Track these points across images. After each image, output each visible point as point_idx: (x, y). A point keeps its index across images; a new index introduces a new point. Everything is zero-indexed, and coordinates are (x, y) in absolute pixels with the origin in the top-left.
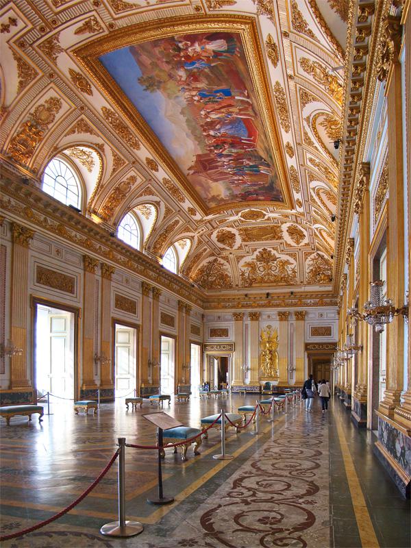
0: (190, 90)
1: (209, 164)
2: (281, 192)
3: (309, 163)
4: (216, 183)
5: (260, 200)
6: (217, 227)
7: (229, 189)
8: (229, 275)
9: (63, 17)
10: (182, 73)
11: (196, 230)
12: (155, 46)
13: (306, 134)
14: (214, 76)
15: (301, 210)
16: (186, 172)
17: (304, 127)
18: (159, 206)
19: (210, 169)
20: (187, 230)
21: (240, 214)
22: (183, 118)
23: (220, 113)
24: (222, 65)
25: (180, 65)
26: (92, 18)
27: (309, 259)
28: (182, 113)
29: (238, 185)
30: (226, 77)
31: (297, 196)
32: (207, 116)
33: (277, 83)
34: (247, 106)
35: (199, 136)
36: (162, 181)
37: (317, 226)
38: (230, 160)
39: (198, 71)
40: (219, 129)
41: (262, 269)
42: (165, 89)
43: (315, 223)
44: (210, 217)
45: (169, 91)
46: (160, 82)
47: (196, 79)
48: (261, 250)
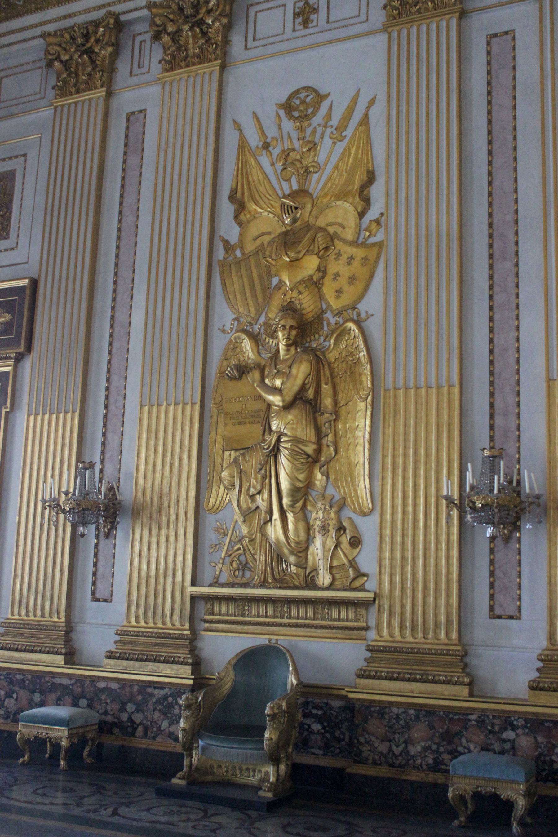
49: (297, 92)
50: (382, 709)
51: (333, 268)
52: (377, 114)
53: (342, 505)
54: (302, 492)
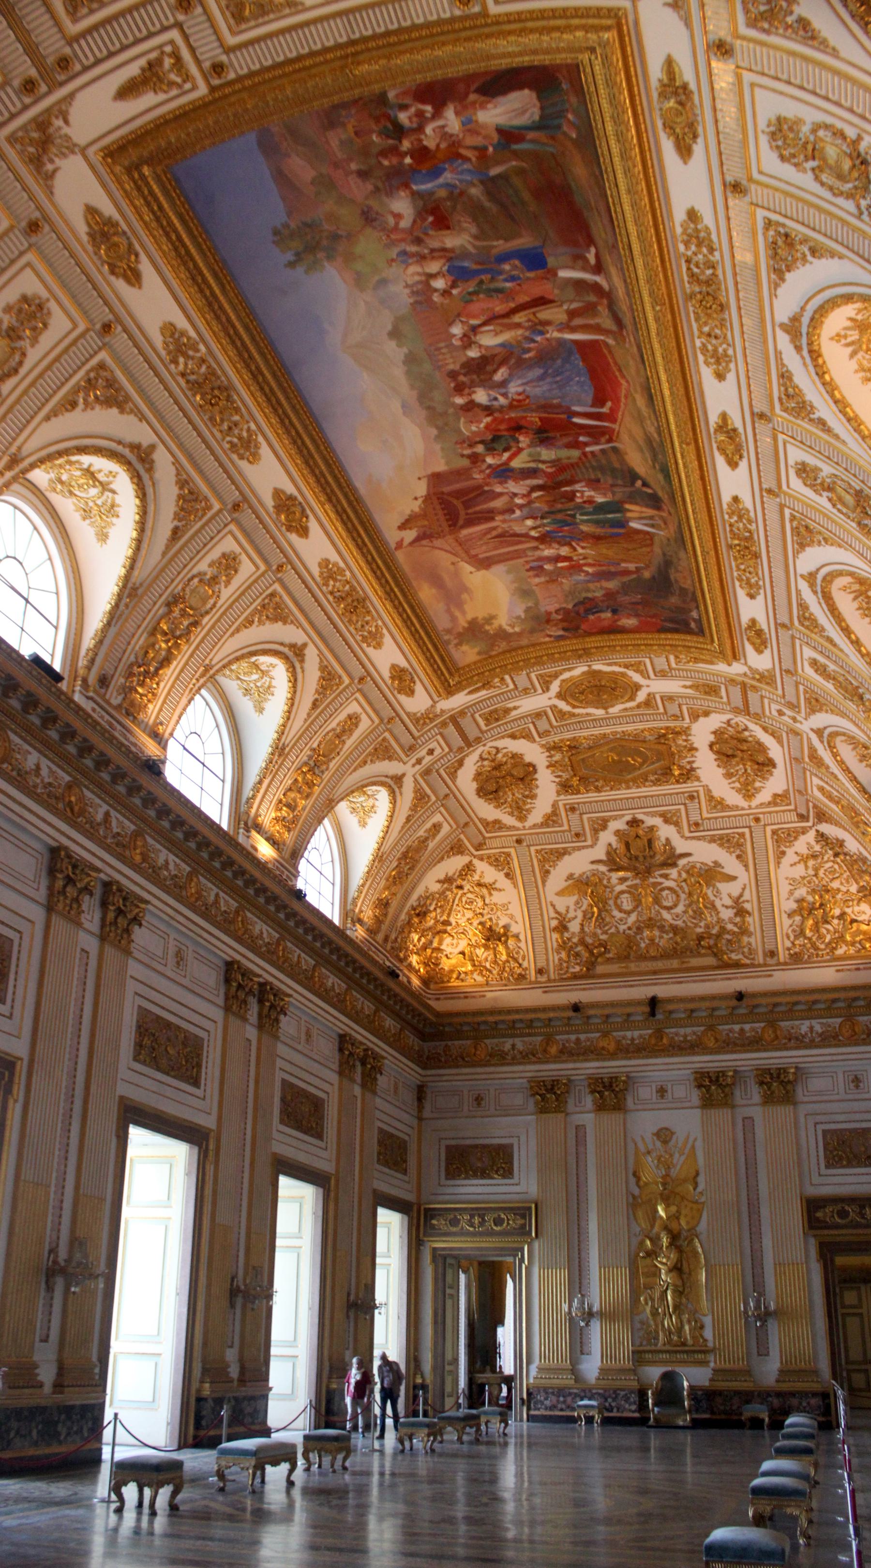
0: (422, 258)
1: (467, 505)
2: (694, 599)
3: (796, 483)
4: (483, 572)
5: (623, 630)
6: (478, 740)
7: (525, 593)
8: (514, 929)
9: (87, 50)
10: (402, 206)
11: (412, 748)
13: (785, 376)
14: (499, 207)
15: (761, 661)
16: (391, 535)
17: (778, 354)
18: (302, 661)
19: (470, 523)
20: (383, 752)
21: (555, 687)
22: (395, 352)
23: (518, 326)
24: (521, 172)
25: (398, 179)
26: (168, 49)
27: (790, 856)
28: (395, 334)
29: (553, 579)
30: (533, 207)
31: (750, 609)
32: (468, 341)
33: (692, 215)
34: (592, 298)
35: (440, 409)
36: (316, 571)
37: (821, 719)
38: (533, 489)
39: (451, 196)
40: (504, 384)
41: (626, 902)
42: (350, 258)
43: (813, 711)
44: (460, 700)
45: (359, 266)
46: (335, 237)
47: (442, 223)
48: (619, 825)
49: (661, 1129)
50: (720, 1393)
51: (683, 1212)
52: (699, 1144)
53: (696, 1311)
54: (676, 1307)
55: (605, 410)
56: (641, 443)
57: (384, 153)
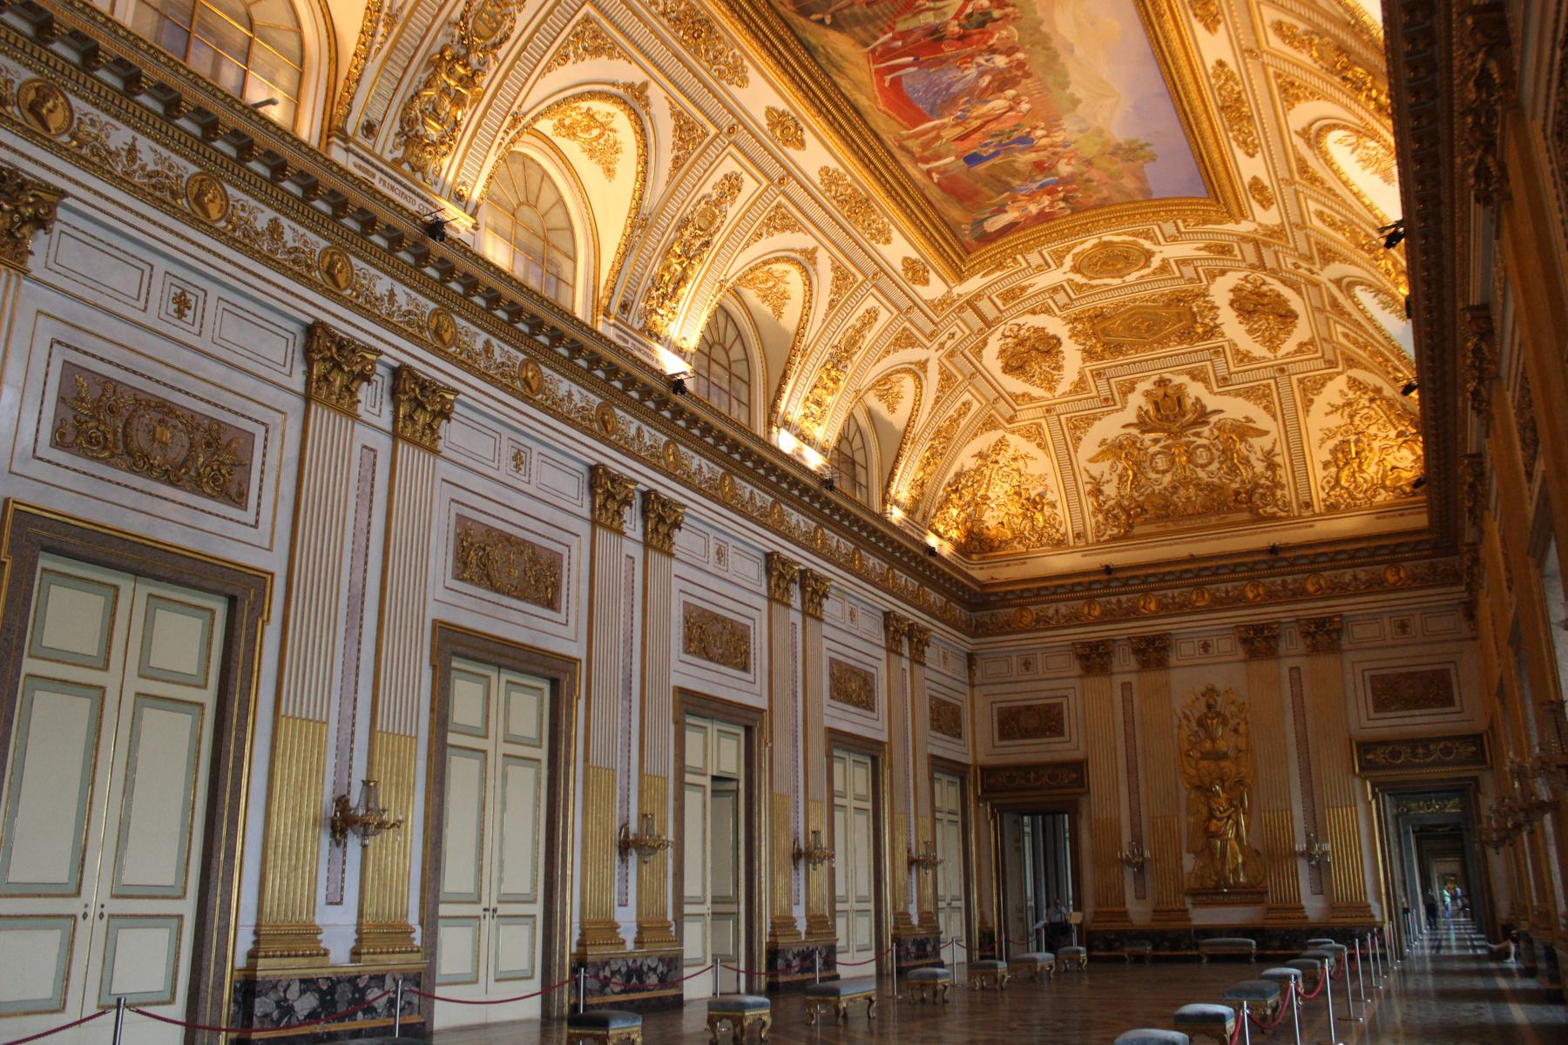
12: (1105, 199)
22: (1076, 90)
23: (976, 118)
24: (990, 198)
25: (1064, 181)
28: (1076, 102)
30: (979, 186)
34: (927, 154)
35: (1038, 48)
40: (982, 74)
46: (1113, 154)
47: (1039, 166)
55: (888, 78)
56: (845, 64)
57: (1076, 190)
